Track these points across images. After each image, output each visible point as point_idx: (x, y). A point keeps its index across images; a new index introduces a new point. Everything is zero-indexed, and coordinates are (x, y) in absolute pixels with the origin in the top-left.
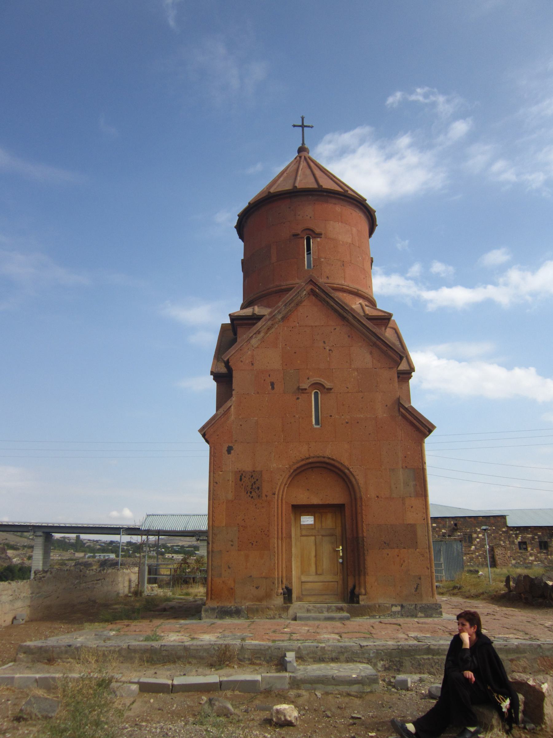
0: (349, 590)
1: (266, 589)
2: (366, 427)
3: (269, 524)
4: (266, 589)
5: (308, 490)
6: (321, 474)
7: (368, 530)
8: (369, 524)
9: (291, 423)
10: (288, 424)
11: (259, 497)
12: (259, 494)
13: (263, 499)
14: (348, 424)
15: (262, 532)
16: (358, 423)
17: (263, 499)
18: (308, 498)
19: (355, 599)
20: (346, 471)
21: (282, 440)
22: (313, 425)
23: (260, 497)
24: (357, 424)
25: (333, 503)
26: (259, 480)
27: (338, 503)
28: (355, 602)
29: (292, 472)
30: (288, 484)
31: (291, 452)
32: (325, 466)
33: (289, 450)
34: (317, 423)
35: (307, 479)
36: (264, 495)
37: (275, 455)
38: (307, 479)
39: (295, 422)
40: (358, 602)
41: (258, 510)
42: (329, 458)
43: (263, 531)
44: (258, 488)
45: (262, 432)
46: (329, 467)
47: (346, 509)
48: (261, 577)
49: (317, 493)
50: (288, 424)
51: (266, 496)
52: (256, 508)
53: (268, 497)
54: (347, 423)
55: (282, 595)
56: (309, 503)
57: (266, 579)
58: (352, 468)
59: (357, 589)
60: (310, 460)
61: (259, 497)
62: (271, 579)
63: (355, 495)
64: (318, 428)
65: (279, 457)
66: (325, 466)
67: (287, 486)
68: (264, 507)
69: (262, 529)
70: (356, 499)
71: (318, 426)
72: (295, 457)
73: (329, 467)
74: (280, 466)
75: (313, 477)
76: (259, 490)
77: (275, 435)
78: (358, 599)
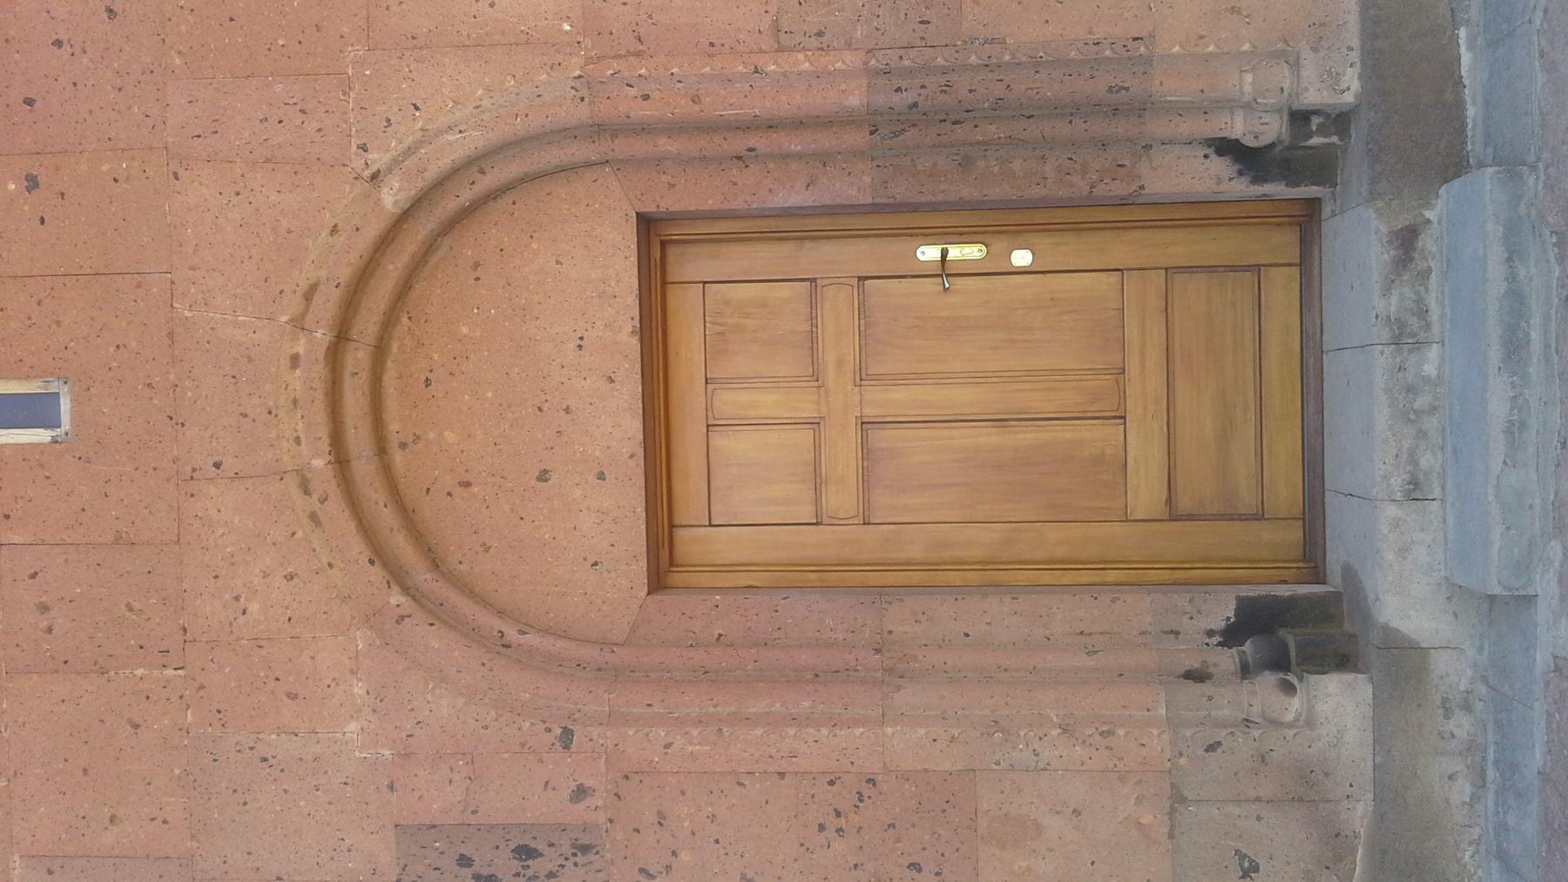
0: (1241, 188)
1: (1258, 799)
2: (58, 43)
3: (782, 775)
4: (1258, 799)
5: (543, 476)
6: (428, 382)
7: (820, 34)
8: (776, 28)
9: (44, 608)
10: (50, 630)
11: (585, 849)
12: (567, 849)
13: (601, 818)
14: (42, 180)
15: (839, 830)
16: (29, 102)
17: (601, 818)
18: (601, 476)
19: (1315, 141)
20: (392, 197)
21: (170, 672)
22: (55, 441)
23: (585, 840)
24: (37, 105)
25: (632, 300)
26: (467, 850)
27: (634, 259)
28: (1335, 139)
29: (403, 599)
30: (498, 624)
31: (254, 607)
32: (357, 358)
33: (242, 619)
34: (36, 411)
35: (467, 484)
36: (579, 812)
37: (280, 730)
38: (467, 484)
39: (33, 576)
40: (1340, 121)
41: (684, 856)
42: (298, 324)
43: (832, 823)
44: (526, 853)
45: (113, 819)
46: (367, 325)
47: (669, 203)
48: (1171, 836)
49: (567, 410)
50: (50, 630)
51: (581, 792)
52: (669, 868)
53: (589, 783)
54: (32, 183)
55: (1291, 678)
56: (637, 469)
57: (1183, 800)
58: (364, 148)
59: (1238, 127)
60: (318, 463)
61: (585, 849)
62: (1183, 761)
63: (566, 133)
64: (76, 401)
65: (293, 696)
66: (357, 358)
67: (512, 634)
68: (661, 815)
69: (822, 828)
70: (599, 130)
71: (65, 405)
72: (290, 577)
73: (367, 325)
74: (359, 689)
75: (450, 436)
76: (541, 846)
77: (136, 726)
78: (1316, 121)
